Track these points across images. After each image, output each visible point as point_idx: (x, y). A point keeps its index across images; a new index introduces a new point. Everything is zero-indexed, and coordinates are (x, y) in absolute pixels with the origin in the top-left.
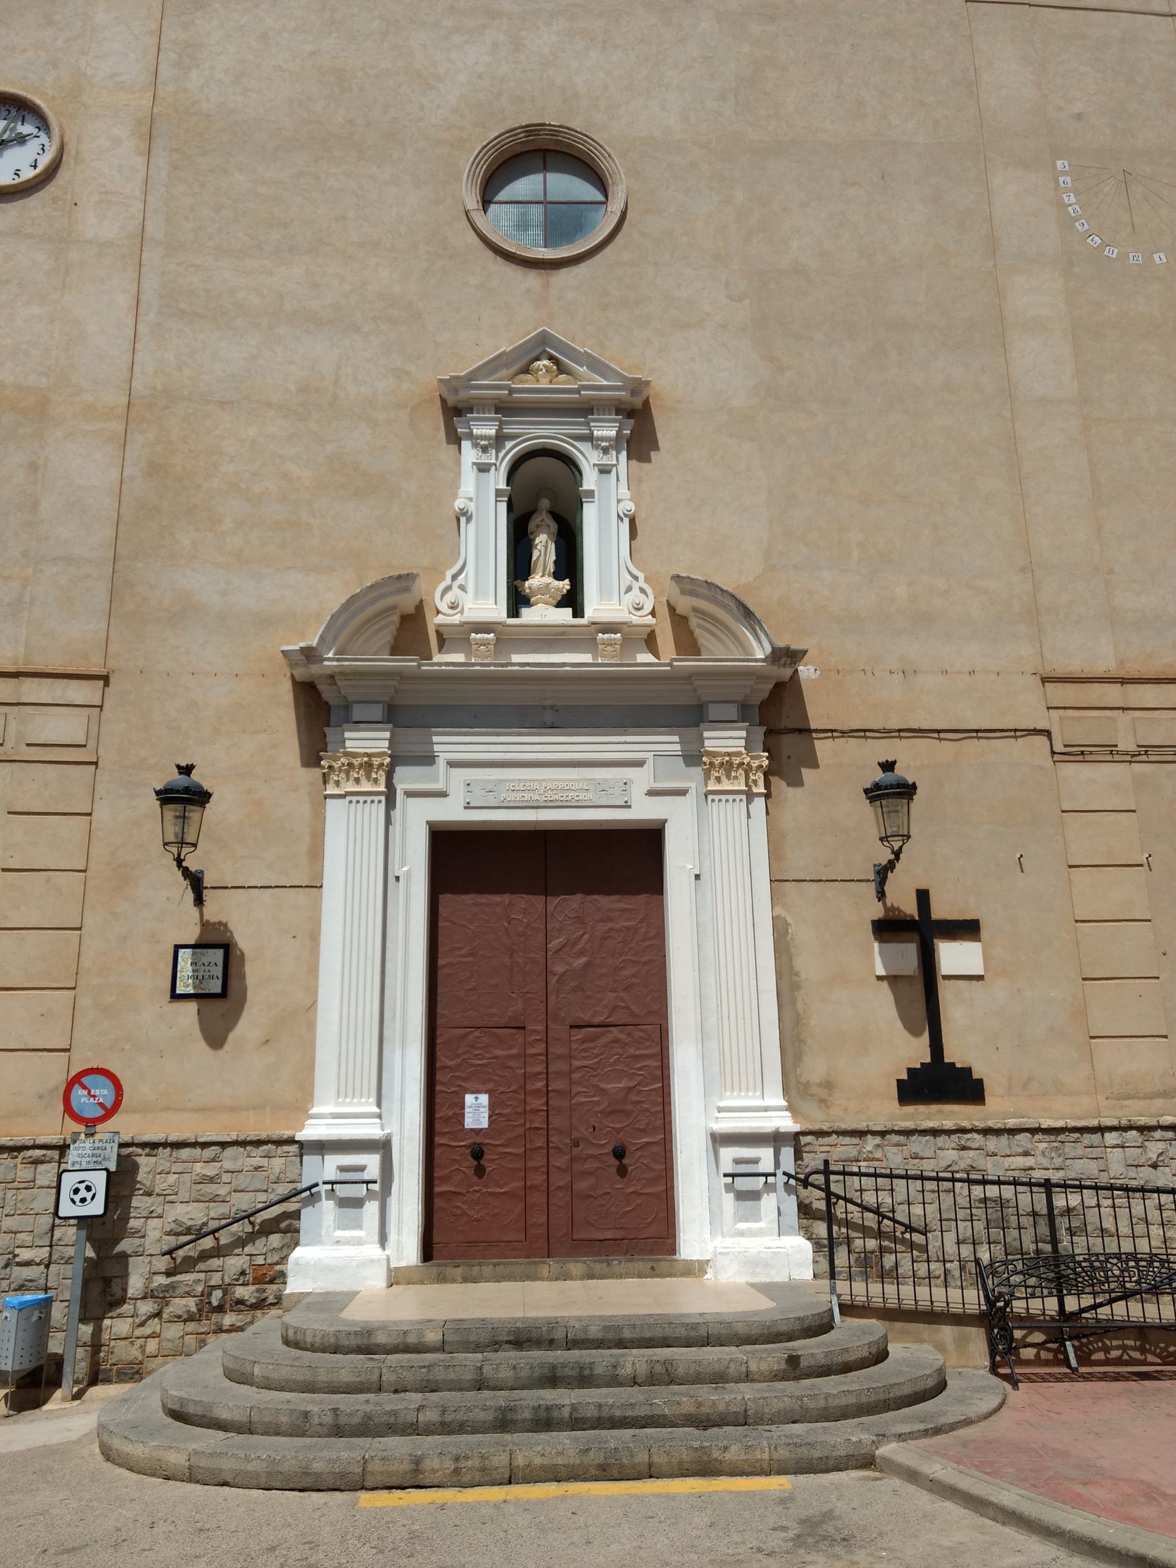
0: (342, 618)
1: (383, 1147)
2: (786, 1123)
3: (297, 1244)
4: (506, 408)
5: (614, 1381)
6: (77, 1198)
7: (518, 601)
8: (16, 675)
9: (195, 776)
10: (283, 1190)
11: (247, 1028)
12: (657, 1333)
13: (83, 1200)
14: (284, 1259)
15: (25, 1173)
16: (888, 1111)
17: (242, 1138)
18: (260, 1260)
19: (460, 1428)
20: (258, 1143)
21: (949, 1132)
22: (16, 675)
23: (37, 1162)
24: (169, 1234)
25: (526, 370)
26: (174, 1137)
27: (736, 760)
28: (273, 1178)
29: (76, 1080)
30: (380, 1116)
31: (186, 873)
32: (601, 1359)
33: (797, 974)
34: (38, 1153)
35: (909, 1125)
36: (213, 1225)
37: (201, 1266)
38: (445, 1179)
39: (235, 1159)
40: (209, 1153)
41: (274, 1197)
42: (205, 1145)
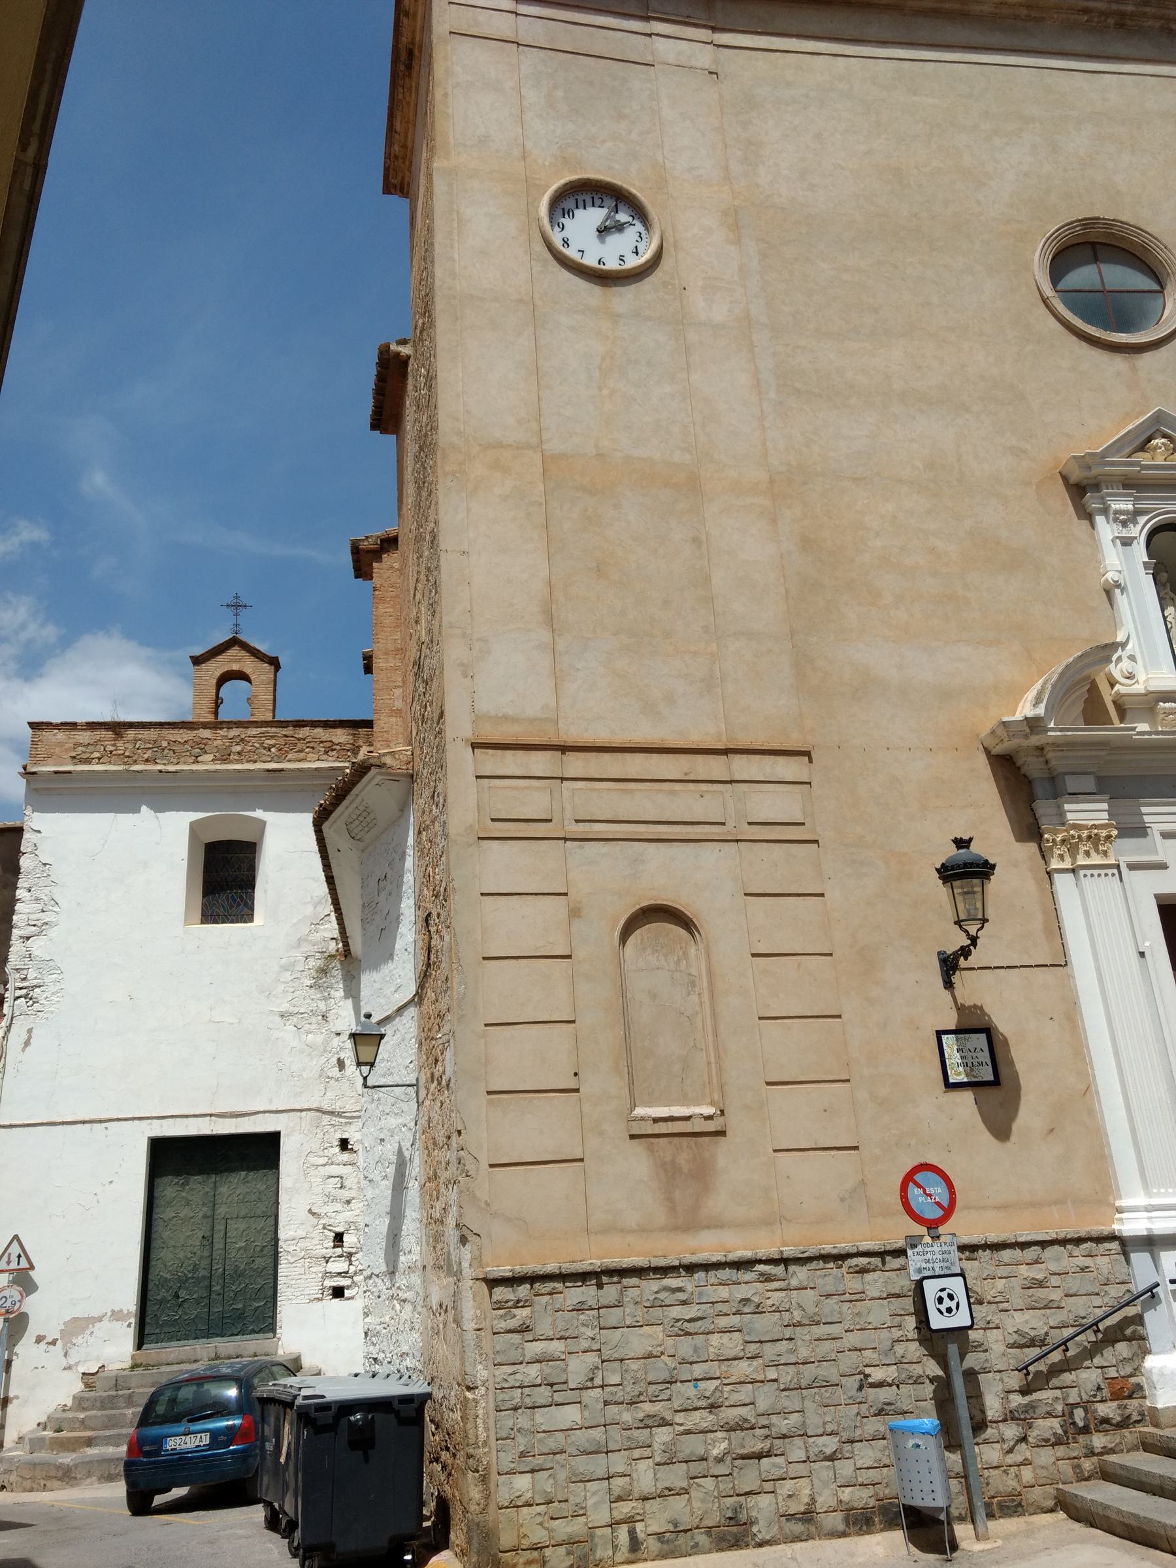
3: (1146, 1352)
4: (1133, 484)
6: (943, 1308)
8: (725, 752)
9: (974, 848)
10: (1115, 1291)
11: (1030, 1116)
13: (949, 1310)
14: (1137, 1371)
15: (853, 1283)
17: (1061, 1236)
18: (1112, 1373)
22: (725, 752)
23: (863, 1271)
24: (1012, 1346)
25: (1142, 448)
26: (993, 1237)
29: (909, 1179)
37: (1055, 1382)
39: (1058, 1259)
40: (1032, 1253)
42: (1024, 1246)
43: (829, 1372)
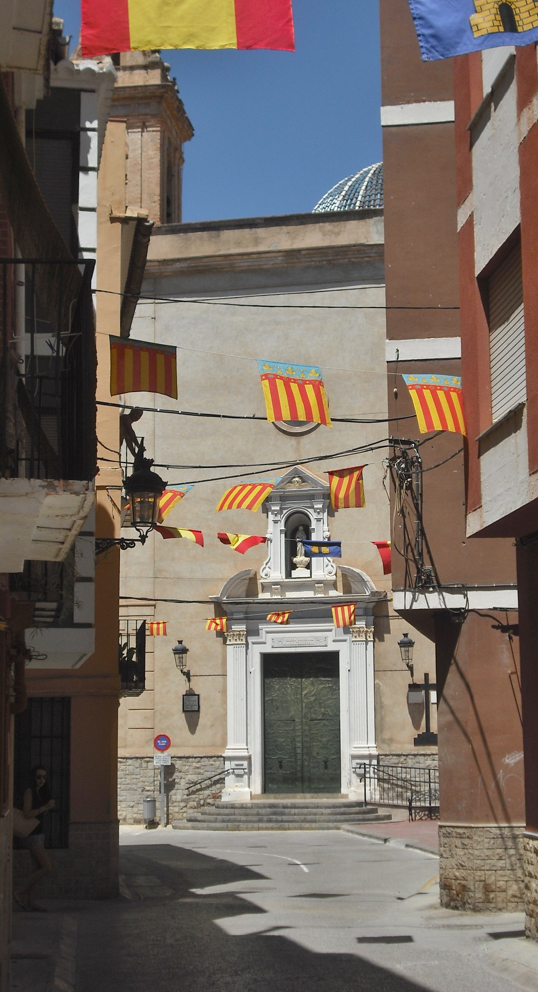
0: (228, 586)
1: (249, 759)
2: (375, 752)
5: (290, 814)
7: (291, 566)
10: (219, 771)
12: (304, 805)
14: (221, 792)
16: (410, 748)
17: (207, 755)
18: (214, 792)
19: (251, 821)
20: (211, 757)
21: (429, 755)
23: (148, 762)
24: (187, 783)
25: (290, 482)
27: (362, 630)
28: (216, 767)
30: (248, 749)
31: (184, 673)
32: (287, 811)
33: (382, 703)
34: (148, 759)
35: (416, 753)
36: (200, 781)
37: (197, 793)
38: (271, 768)
40: (197, 760)
41: (217, 773)
42: (196, 758)
43: (134, 787)
